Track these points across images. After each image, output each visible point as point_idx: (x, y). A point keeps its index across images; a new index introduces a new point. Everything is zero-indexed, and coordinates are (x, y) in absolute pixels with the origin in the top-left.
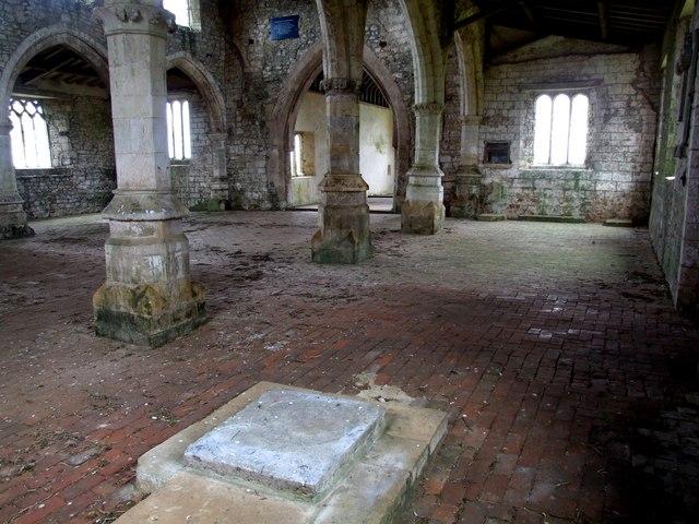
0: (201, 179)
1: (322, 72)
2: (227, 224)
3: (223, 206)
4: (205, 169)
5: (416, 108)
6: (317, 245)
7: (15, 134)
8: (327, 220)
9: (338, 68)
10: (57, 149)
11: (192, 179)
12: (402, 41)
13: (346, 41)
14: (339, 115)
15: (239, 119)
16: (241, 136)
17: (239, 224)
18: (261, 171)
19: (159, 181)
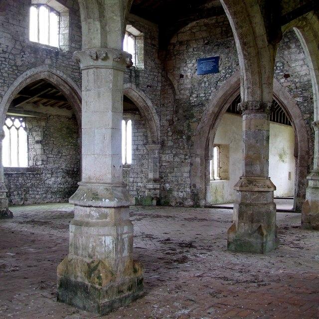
0: (139, 180)
1: (240, 95)
2: (158, 216)
3: (155, 202)
5: (315, 124)
6: (232, 236)
7: (5, 142)
8: (241, 215)
9: (253, 94)
10: (33, 153)
11: (131, 180)
12: (303, 73)
13: (260, 73)
14: (253, 130)
15: (170, 134)
16: (172, 147)
17: (168, 217)
18: (186, 175)
19: (114, 176)
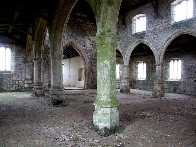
0: (20, 79)
4: (21, 75)
11: (14, 79)
